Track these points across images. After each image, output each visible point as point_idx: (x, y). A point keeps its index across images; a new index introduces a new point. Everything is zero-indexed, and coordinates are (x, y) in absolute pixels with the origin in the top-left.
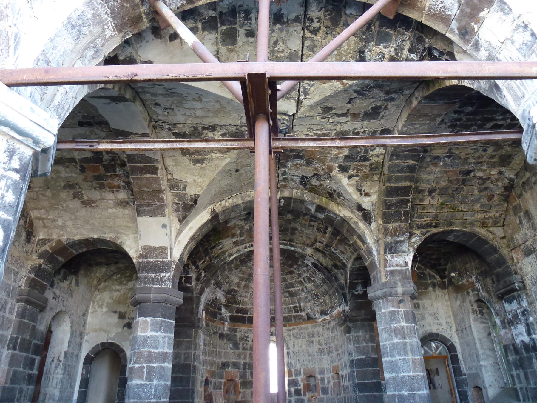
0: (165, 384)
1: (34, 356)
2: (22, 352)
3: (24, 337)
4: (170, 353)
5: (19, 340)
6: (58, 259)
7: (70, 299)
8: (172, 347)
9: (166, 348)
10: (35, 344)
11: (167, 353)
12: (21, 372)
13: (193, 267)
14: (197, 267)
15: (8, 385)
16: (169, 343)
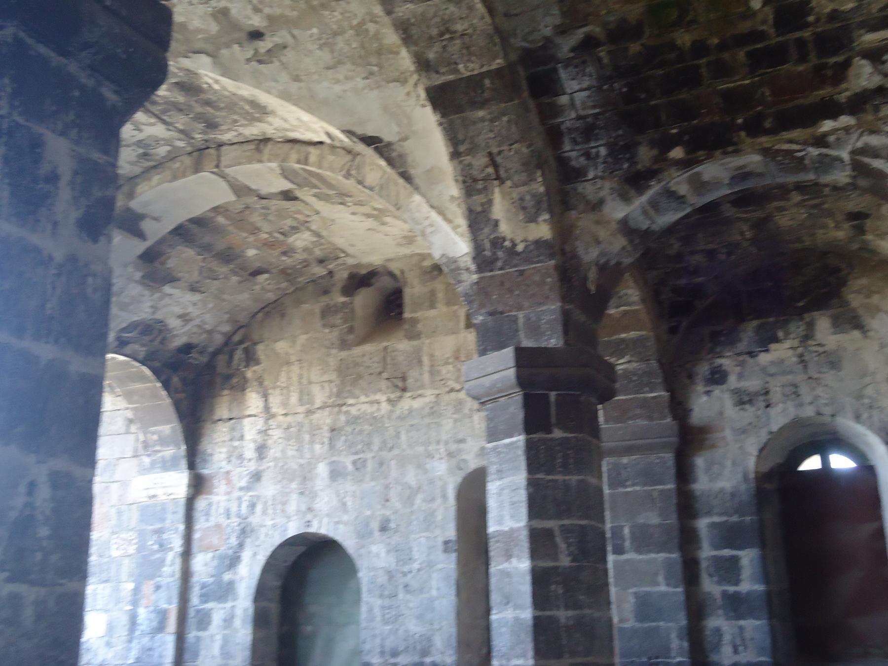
0: (517, 619)
1: (727, 552)
2: (650, 552)
3: (641, 520)
4: (519, 529)
5: (626, 531)
6: (623, 340)
7: (829, 377)
8: (523, 511)
9: (507, 517)
10: (713, 525)
11: (512, 531)
12: (663, 595)
13: (827, 125)
14: (859, 104)
15: (628, 625)
16: (513, 503)
